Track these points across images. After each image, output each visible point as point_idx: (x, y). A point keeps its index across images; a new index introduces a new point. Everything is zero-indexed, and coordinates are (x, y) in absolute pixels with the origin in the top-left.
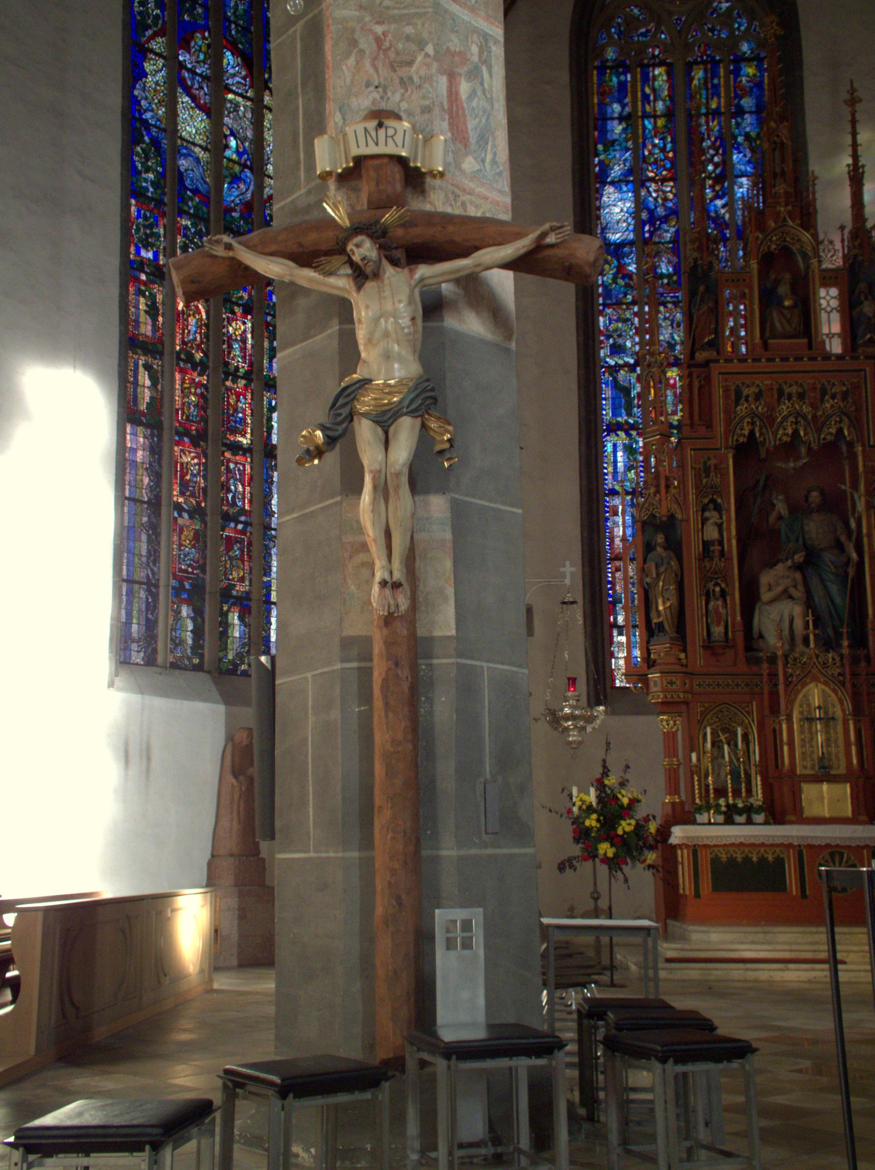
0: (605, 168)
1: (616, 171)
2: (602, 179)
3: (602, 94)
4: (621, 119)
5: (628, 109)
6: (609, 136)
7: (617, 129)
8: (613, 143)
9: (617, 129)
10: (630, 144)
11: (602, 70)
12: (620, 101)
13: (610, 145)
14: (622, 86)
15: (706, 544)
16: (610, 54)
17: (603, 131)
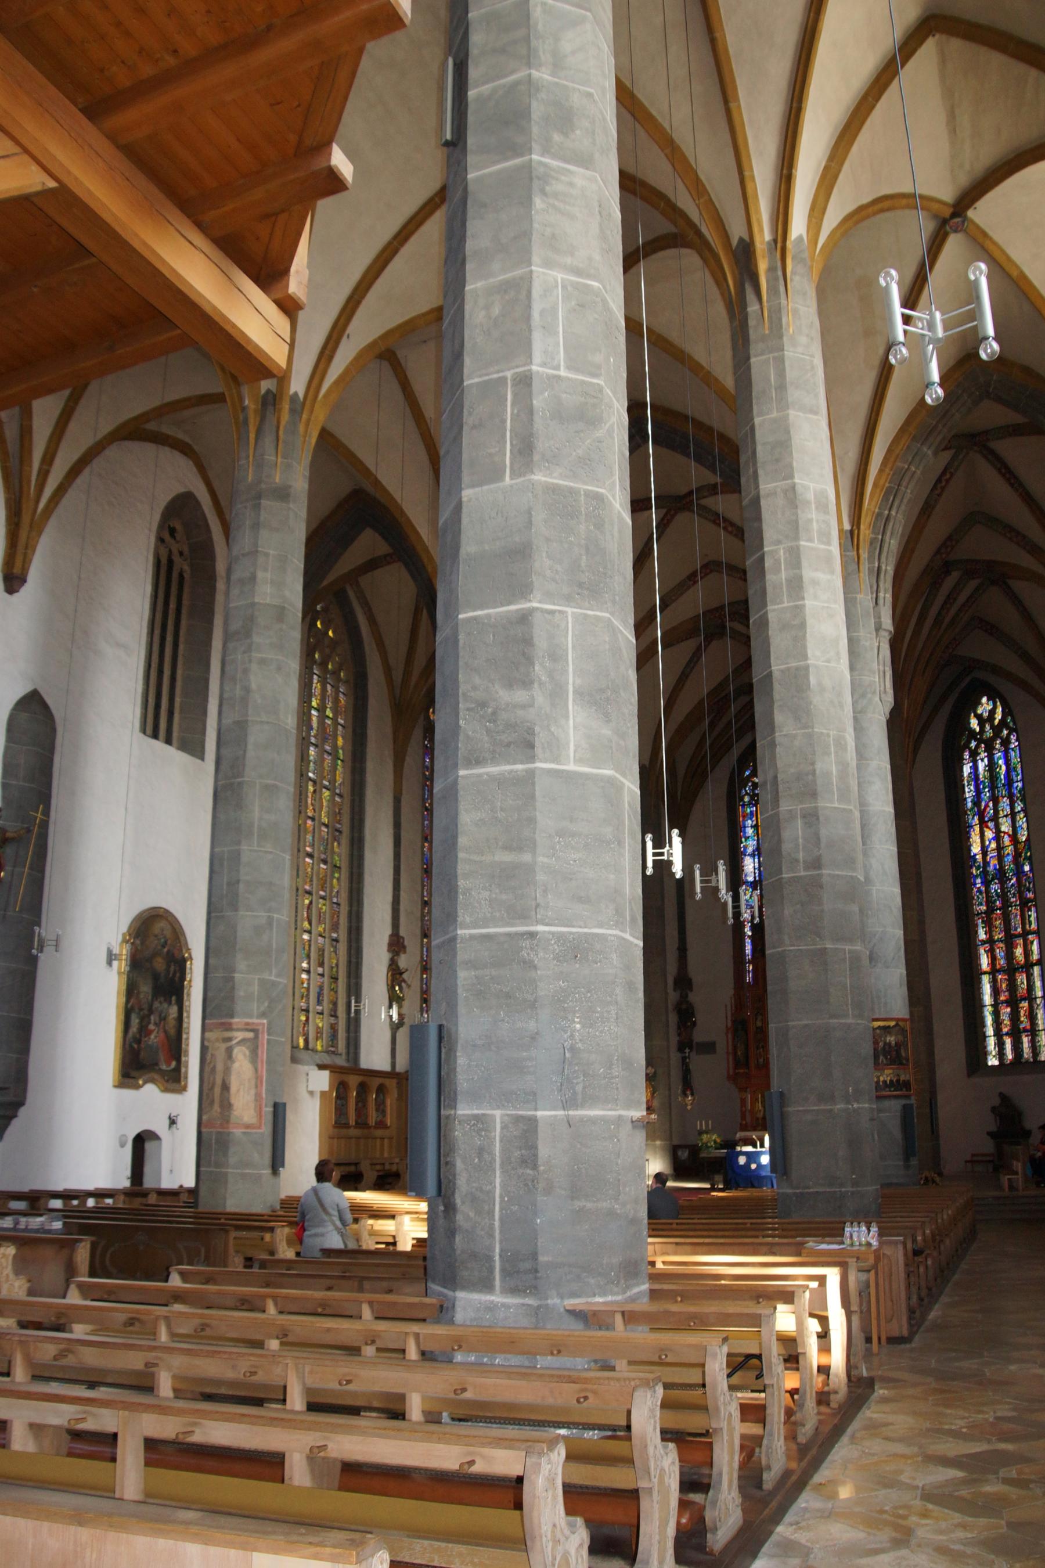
0: (745, 847)
1: (750, 850)
2: (744, 853)
3: (744, 816)
4: (752, 827)
5: (754, 823)
6: (747, 835)
7: (750, 831)
8: (748, 837)
9: (750, 831)
10: (756, 838)
11: (743, 806)
12: (751, 819)
13: (747, 838)
14: (751, 812)
15: (757, 1028)
16: (746, 799)
17: (745, 833)
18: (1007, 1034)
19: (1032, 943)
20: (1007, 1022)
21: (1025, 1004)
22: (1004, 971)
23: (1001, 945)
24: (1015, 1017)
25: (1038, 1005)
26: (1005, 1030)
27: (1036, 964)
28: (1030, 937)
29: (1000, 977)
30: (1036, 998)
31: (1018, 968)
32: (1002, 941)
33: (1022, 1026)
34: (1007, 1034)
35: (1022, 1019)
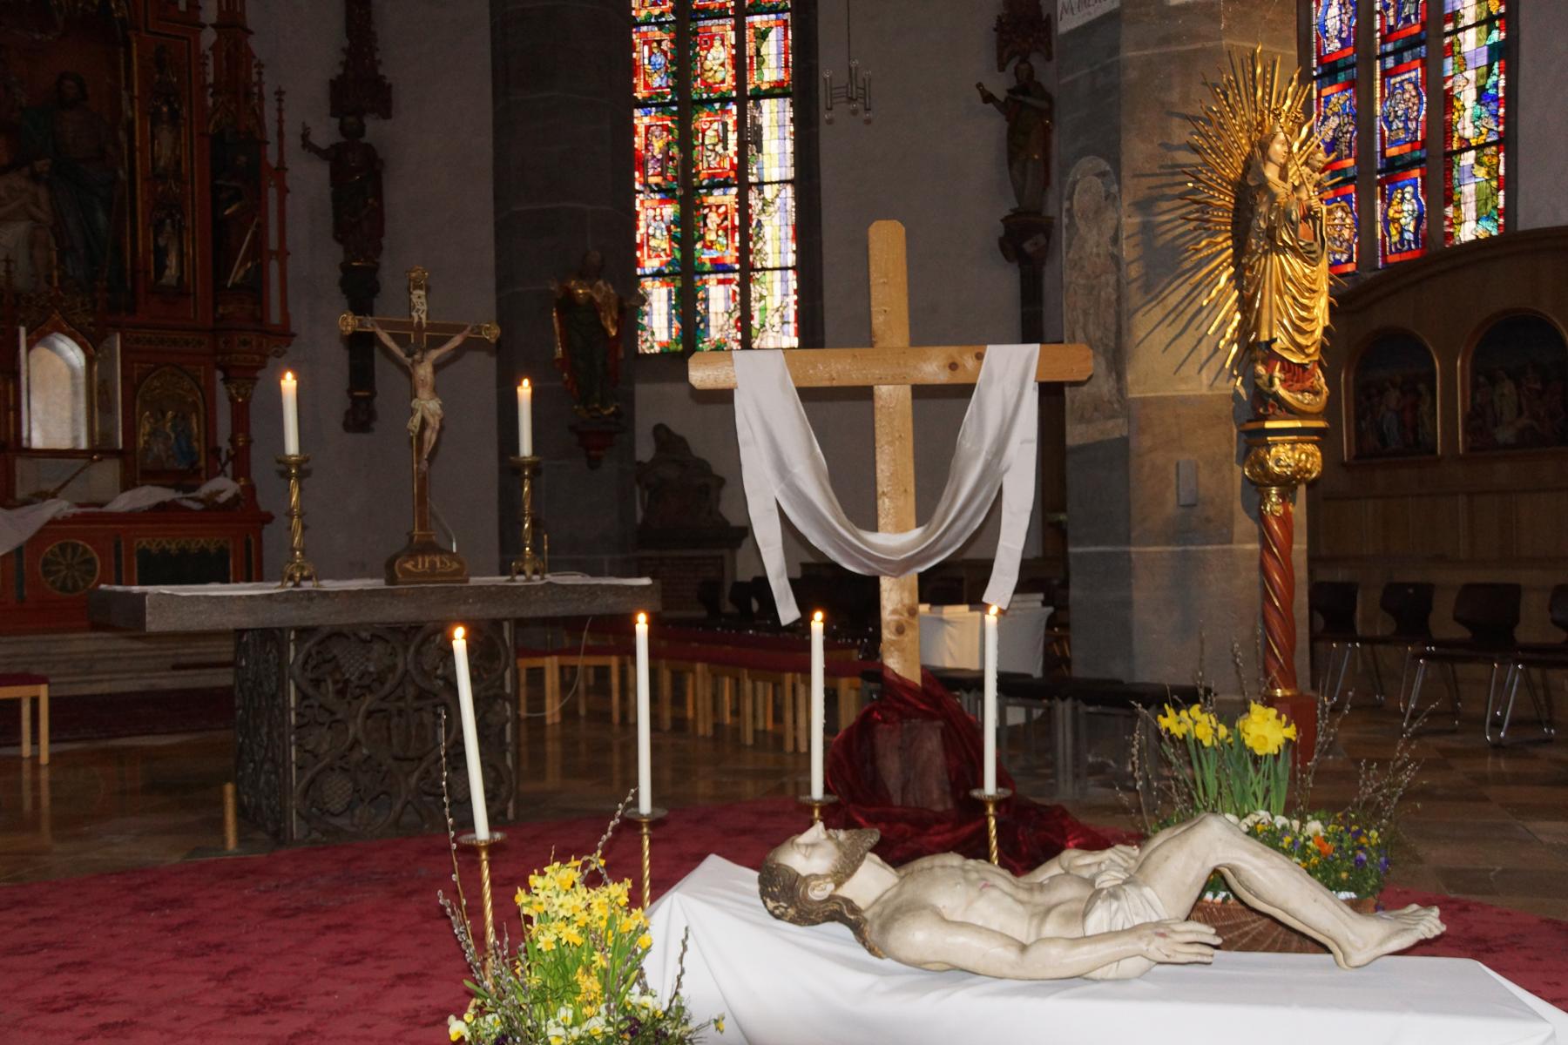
18: (658, 274)
19: (762, 36)
20: (661, 242)
21: (728, 198)
22: (662, 107)
23: (655, 33)
24: (686, 232)
25: (766, 203)
26: (651, 264)
27: (769, 94)
28: (757, 20)
29: (646, 120)
30: (761, 184)
31: (710, 102)
32: (660, 25)
33: (707, 256)
34: (658, 274)
35: (711, 236)
